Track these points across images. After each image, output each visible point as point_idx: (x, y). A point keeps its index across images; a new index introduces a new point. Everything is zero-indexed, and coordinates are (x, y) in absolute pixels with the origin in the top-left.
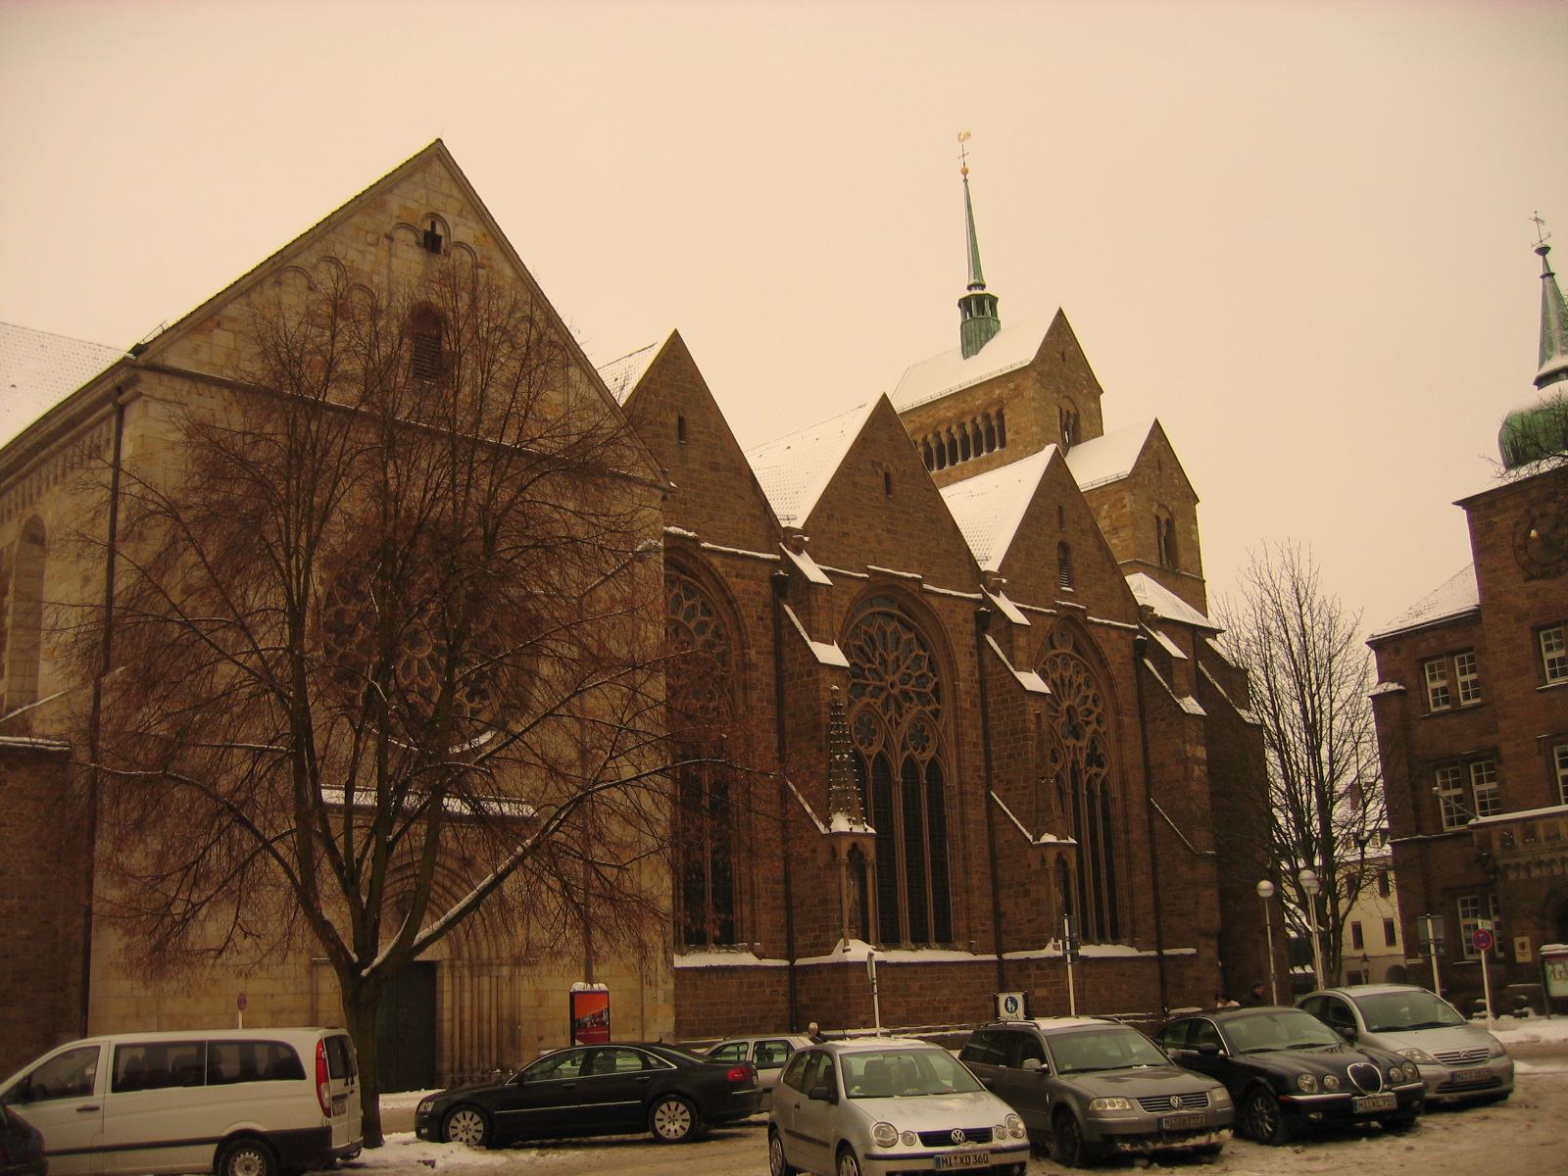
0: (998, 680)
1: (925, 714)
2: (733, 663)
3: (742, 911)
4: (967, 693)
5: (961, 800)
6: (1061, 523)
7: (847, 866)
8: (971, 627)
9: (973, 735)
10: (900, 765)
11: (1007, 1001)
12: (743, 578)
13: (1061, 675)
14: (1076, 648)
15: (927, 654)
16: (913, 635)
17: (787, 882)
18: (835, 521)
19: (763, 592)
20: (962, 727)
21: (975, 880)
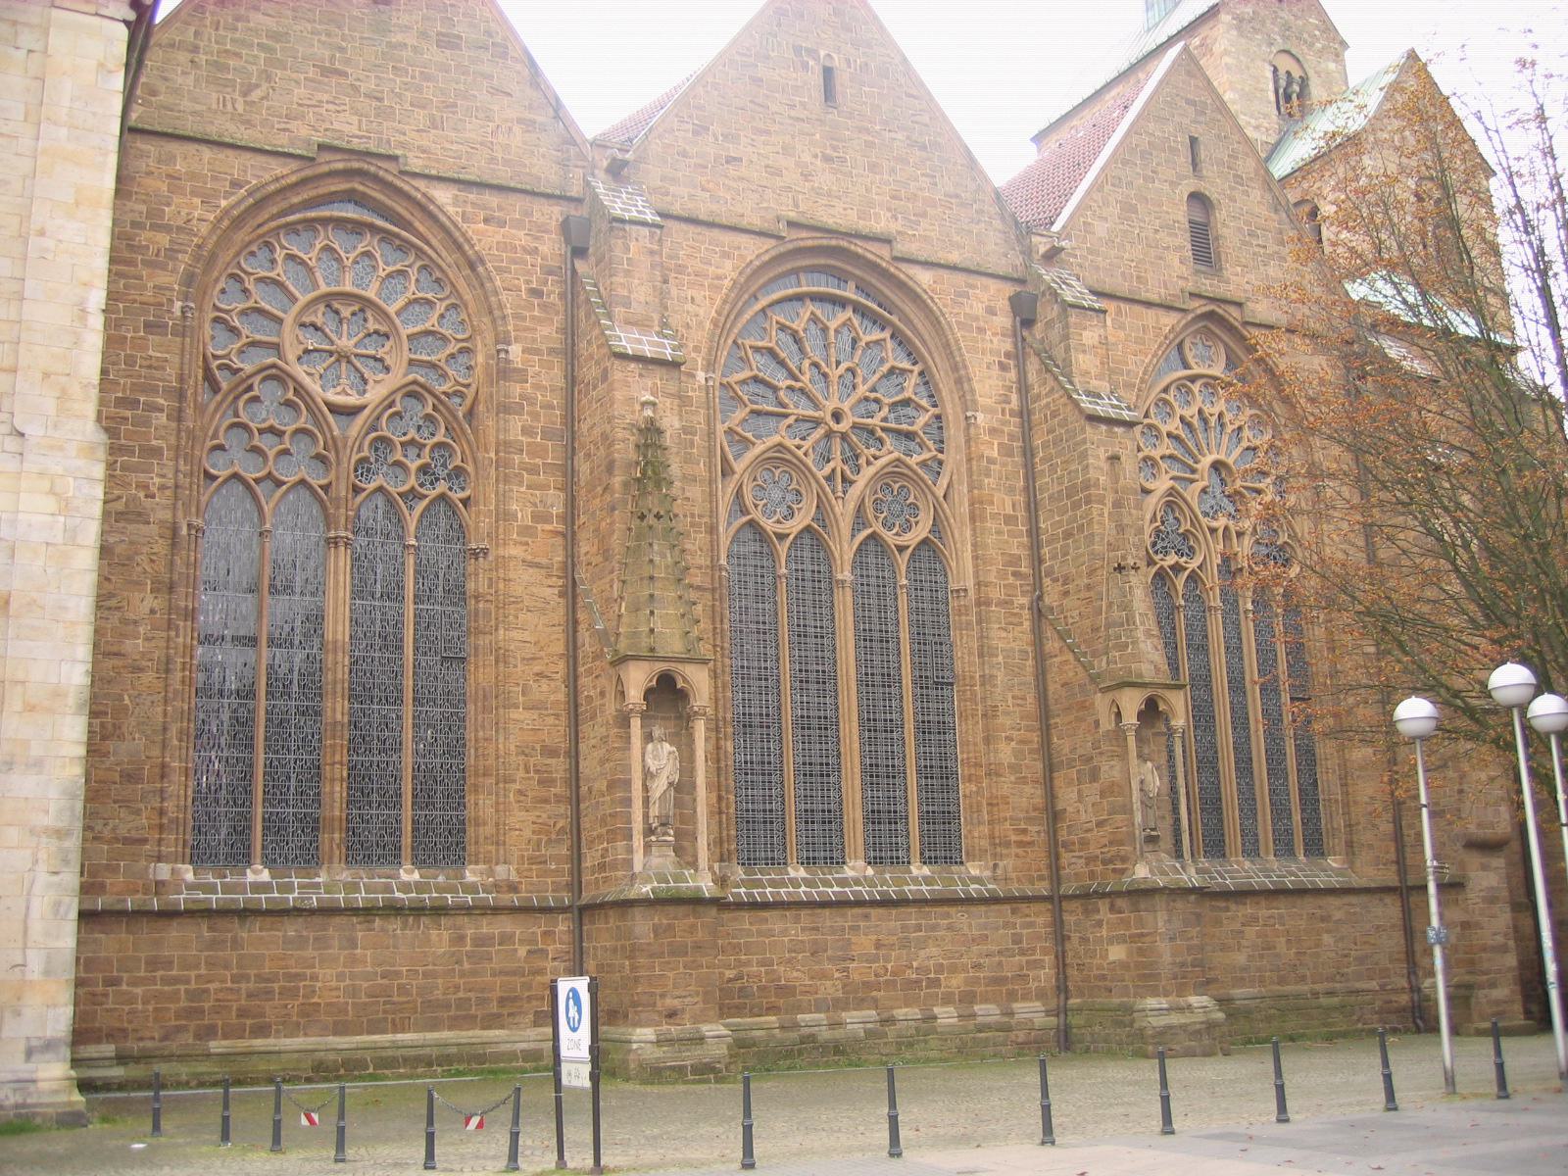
0: (1048, 404)
1: (908, 467)
2: (479, 370)
3: (481, 805)
4: (993, 431)
5: (979, 614)
6: (1195, 164)
7: (644, 716)
8: (1004, 320)
9: (1006, 502)
10: (849, 555)
11: (568, 999)
12: (502, 224)
13: (1200, 412)
14: (1231, 363)
15: (917, 369)
16: (886, 334)
17: (574, 755)
18: (711, 139)
19: (544, 249)
20: (980, 488)
21: (1005, 753)
